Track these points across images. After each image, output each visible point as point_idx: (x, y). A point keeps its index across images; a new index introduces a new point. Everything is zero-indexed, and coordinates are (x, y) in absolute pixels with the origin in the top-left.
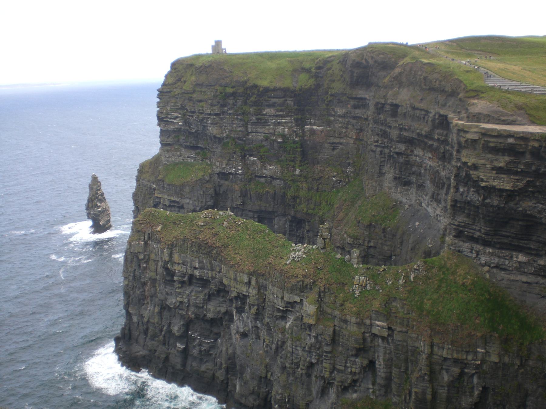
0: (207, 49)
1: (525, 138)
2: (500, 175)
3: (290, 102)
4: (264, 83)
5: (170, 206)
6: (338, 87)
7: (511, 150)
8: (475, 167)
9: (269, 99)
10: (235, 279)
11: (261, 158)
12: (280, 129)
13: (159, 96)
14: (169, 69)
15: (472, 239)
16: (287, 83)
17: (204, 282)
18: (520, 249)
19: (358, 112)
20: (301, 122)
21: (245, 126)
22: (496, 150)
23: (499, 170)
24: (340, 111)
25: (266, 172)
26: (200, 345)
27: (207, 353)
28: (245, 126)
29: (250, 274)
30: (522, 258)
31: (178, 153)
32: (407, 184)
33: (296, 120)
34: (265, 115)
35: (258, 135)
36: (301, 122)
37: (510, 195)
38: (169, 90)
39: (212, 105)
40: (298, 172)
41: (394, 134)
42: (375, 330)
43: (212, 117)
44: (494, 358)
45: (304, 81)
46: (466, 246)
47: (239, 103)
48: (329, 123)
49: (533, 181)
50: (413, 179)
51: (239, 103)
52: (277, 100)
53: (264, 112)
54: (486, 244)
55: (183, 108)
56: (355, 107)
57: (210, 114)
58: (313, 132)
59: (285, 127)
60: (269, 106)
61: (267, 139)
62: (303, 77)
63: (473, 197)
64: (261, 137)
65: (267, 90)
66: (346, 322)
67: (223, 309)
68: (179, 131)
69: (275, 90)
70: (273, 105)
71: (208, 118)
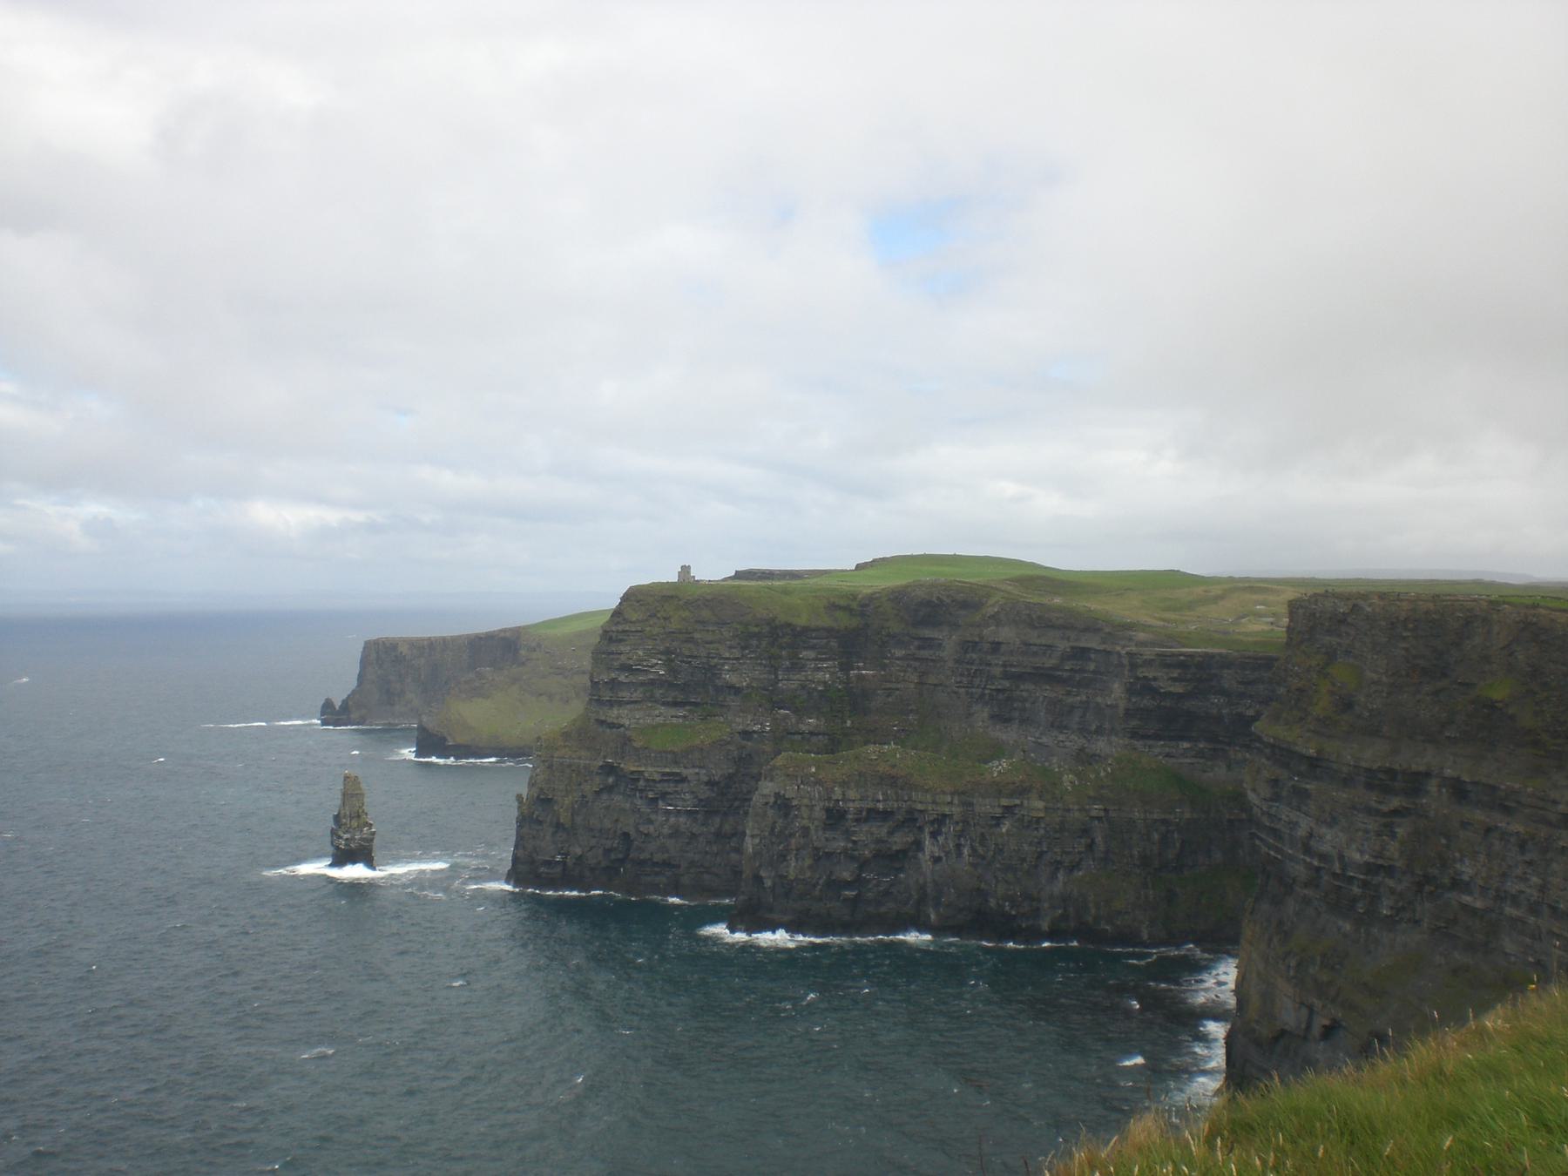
1: (1191, 656)
3: (834, 643)
4: (802, 621)
6: (895, 627)
7: (1183, 665)
8: (1155, 679)
10: (934, 802)
11: (796, 711)
12: (820, 675)
15: (1144, 737)
16: (826, 621)
17: (886, 815)
18: (1182, 738)
19: (925, 653)
20: (846, 667)
22: (1169, 666)
23: (1174, 680)
24: (899, 653)
25: (803, 728)
26: (877, 885)
27: (887, 893)
28: (775, 670)
29: (952, 794)
30: (1186, 745)
32: (1008, 720)
33: (841, 664)
35: (789, 683)
36: (846, 667)
37: (1180, 696)
40: (849, 723)
41: (997, 671)
42: (1094, 813)
44: (1187, 815)
45: (844, 621)
46: (1138, 744)
47: (764, 644)
48: (884, 667)
50: (1016, 714)
51: (764, 644)
54: (1157, 737)
55: (668, 652)
56: (919, 648)
58: (861, 678)
59: (823, 674)
60: (806, 648)
61: (803, 687)
62: (839, 614)
63: (1147, 702)
64: (794, 685)
66: (1069, 810)
67: (910, 839)
69: (817, 629)
70: (813, 648)
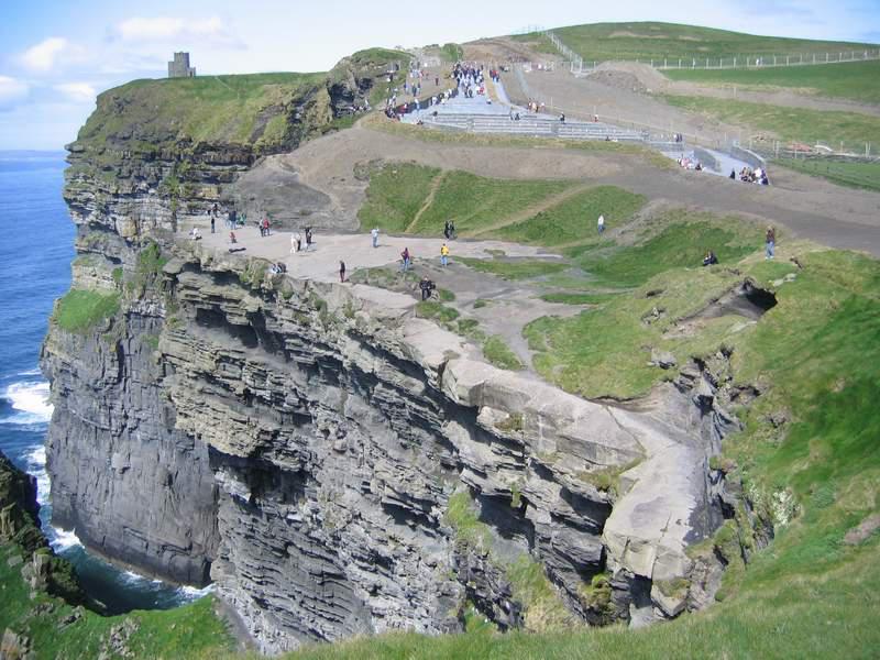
0: (160, 70)
2: (210, 401)
5: (61, 371)
9: (208, 167)
13: (70, 160)
14: (94, 107)
21: (174, 220)
28: (174, 220)
31: (91, 269)
34: (201, 199)
38: (81, 148)
39: (120, 176)
43: (120, 200)
49: (276, 434)
51: (167, 173)
52: (221, 168)
53: (201, 194)
57: (116, 195)
65: (204, 147)
68: (96, 226)
71: (115, 203)
